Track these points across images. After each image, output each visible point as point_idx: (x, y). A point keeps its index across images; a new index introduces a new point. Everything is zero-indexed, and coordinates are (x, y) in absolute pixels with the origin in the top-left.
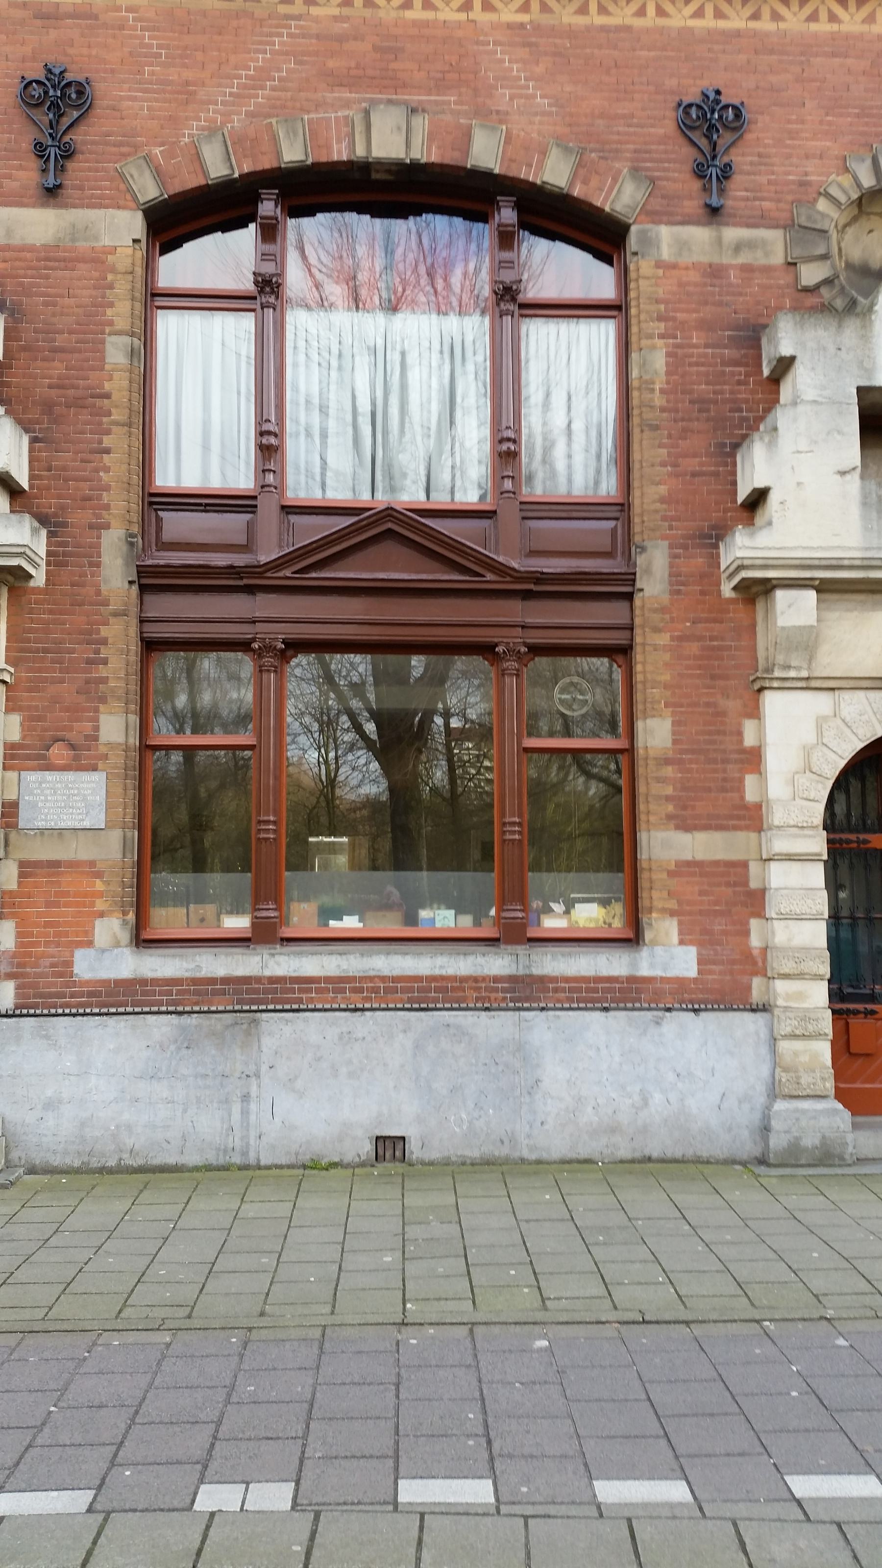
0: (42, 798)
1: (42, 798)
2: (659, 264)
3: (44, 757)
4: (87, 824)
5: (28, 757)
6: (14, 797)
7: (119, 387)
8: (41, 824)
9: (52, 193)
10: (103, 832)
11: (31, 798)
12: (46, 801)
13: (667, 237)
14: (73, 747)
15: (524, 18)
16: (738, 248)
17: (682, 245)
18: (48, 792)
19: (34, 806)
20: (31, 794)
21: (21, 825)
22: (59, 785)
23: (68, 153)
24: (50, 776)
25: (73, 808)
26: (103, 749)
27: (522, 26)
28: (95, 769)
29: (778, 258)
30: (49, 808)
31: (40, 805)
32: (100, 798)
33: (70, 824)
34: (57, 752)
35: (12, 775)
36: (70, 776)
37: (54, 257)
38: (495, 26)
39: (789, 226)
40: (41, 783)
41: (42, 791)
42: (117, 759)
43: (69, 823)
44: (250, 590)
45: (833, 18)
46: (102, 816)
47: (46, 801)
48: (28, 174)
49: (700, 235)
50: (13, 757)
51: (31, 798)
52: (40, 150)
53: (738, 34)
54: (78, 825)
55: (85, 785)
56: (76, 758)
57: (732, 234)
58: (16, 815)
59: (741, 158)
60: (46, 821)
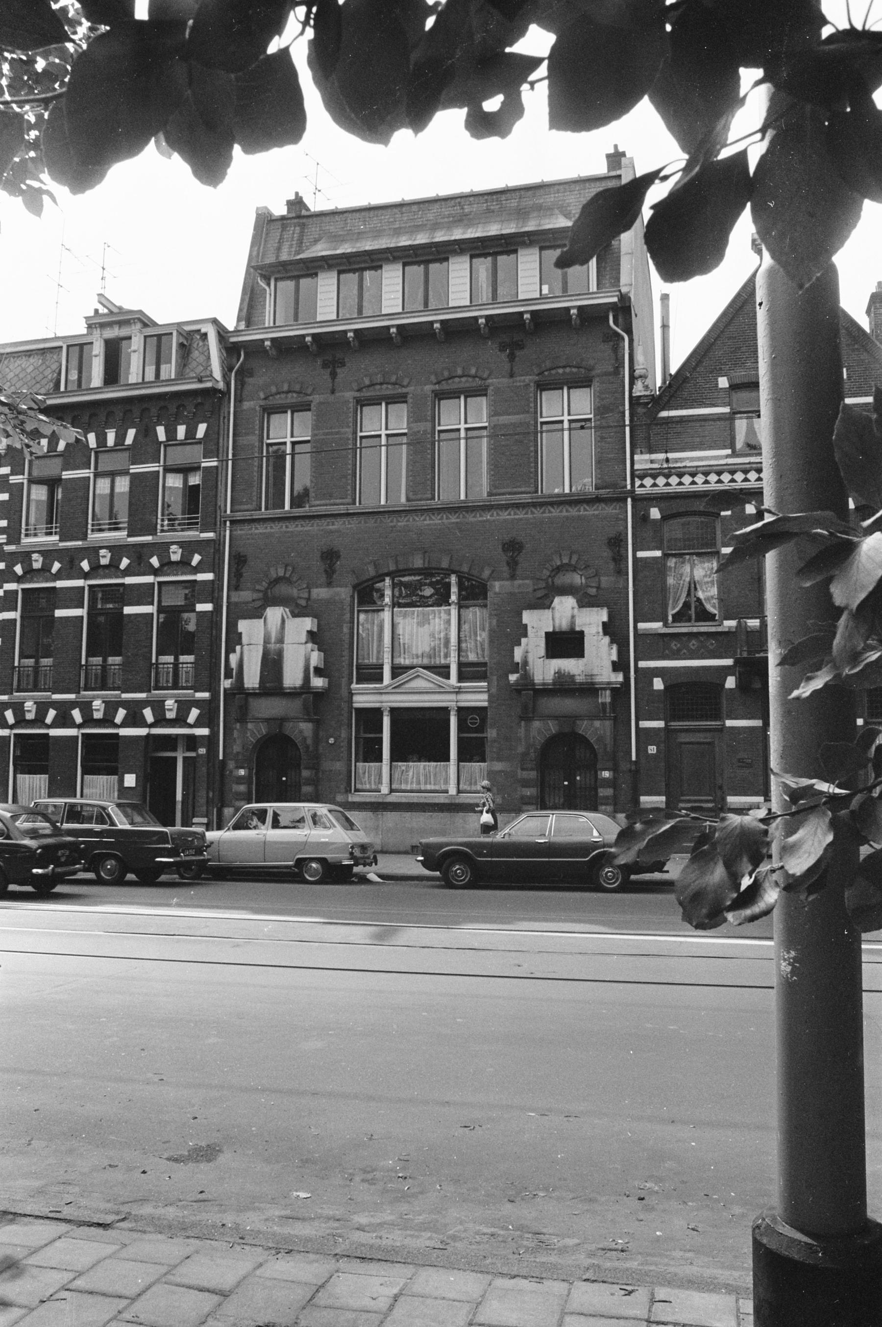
2: (495, 593)
7: (346, 638)
9: (329, 584)
13: (497, 586)
15: (458, 520)
16: (520, 586)
17: (501, 587)
23: (334, 572)
27: (457, 523)
29: (531, 589)
37: (329, 602)
38: (450, 523)
39: (532, 578)
44: (381, 693)
45: (550, 512)
48: (323, 579)
49: (507, 583)
52: (326, 571)
53: (521, 519)
57: (517, 582)
59: (520, 559)
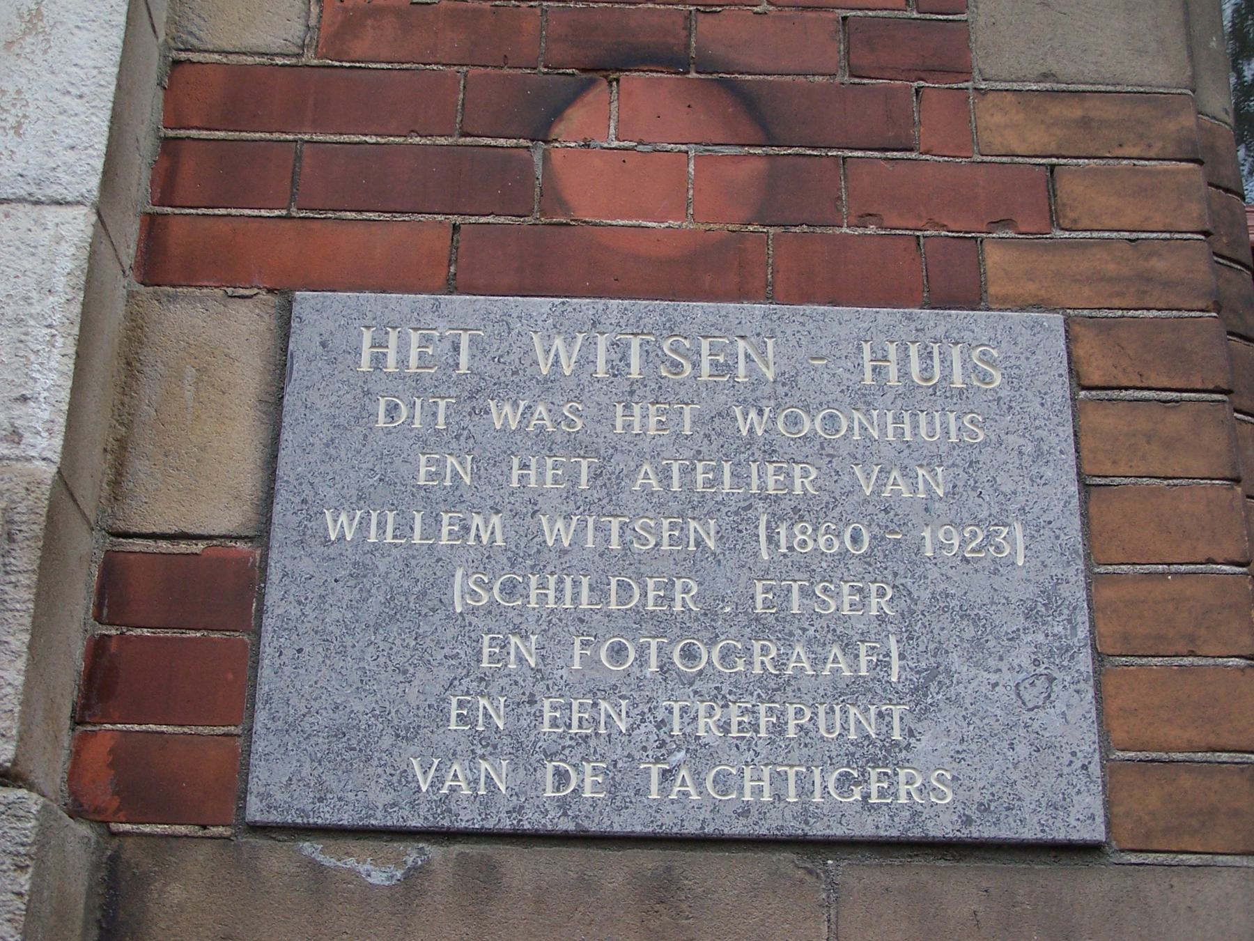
0: (491, 529)
1: (491, 529)
3: (510, 187)
4: (927, 792)
5: (370, 185)
6: (222, 514)
8: (471, 786)
10: (1090, 887)
11: (382, 530)
12: (526, 555)
14: (754, 110)
18: (544, 475)
19: (411, 598)
20: (386, 487)
21: (278, 781)
22: (645, 420)
24: (559, 337)
25: (778, 627)
26: (1006, 130)
28: (958, 290)
30: (552, 626)
31: (463, 590)
32: (1029, 541)
33: (759, 793)
34: (624, 153)
35: (218, 330)
36: (743, 340)
40: (474, 397)
41: (490, 462)
42: (1138, 208)
43: (755, 786)
46: (1071, 719)
47: (526, 555)
50: (234, 177)
51: (382, 530)
54: (837, 807)
55: (884, 426)
56: (776, 203)
58: (230, 689)
60: (519, 747)
